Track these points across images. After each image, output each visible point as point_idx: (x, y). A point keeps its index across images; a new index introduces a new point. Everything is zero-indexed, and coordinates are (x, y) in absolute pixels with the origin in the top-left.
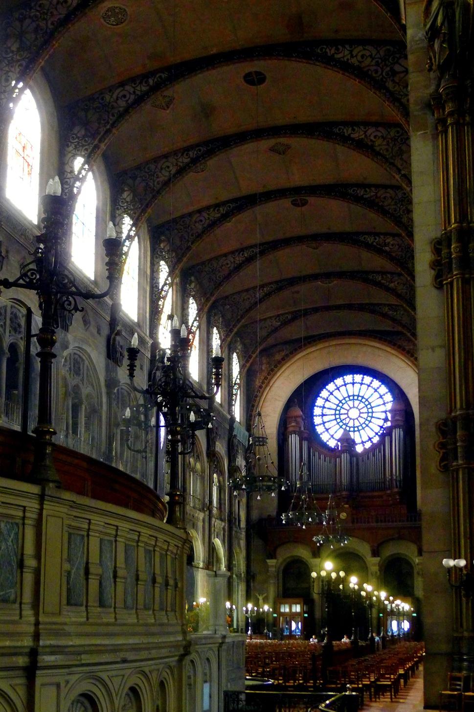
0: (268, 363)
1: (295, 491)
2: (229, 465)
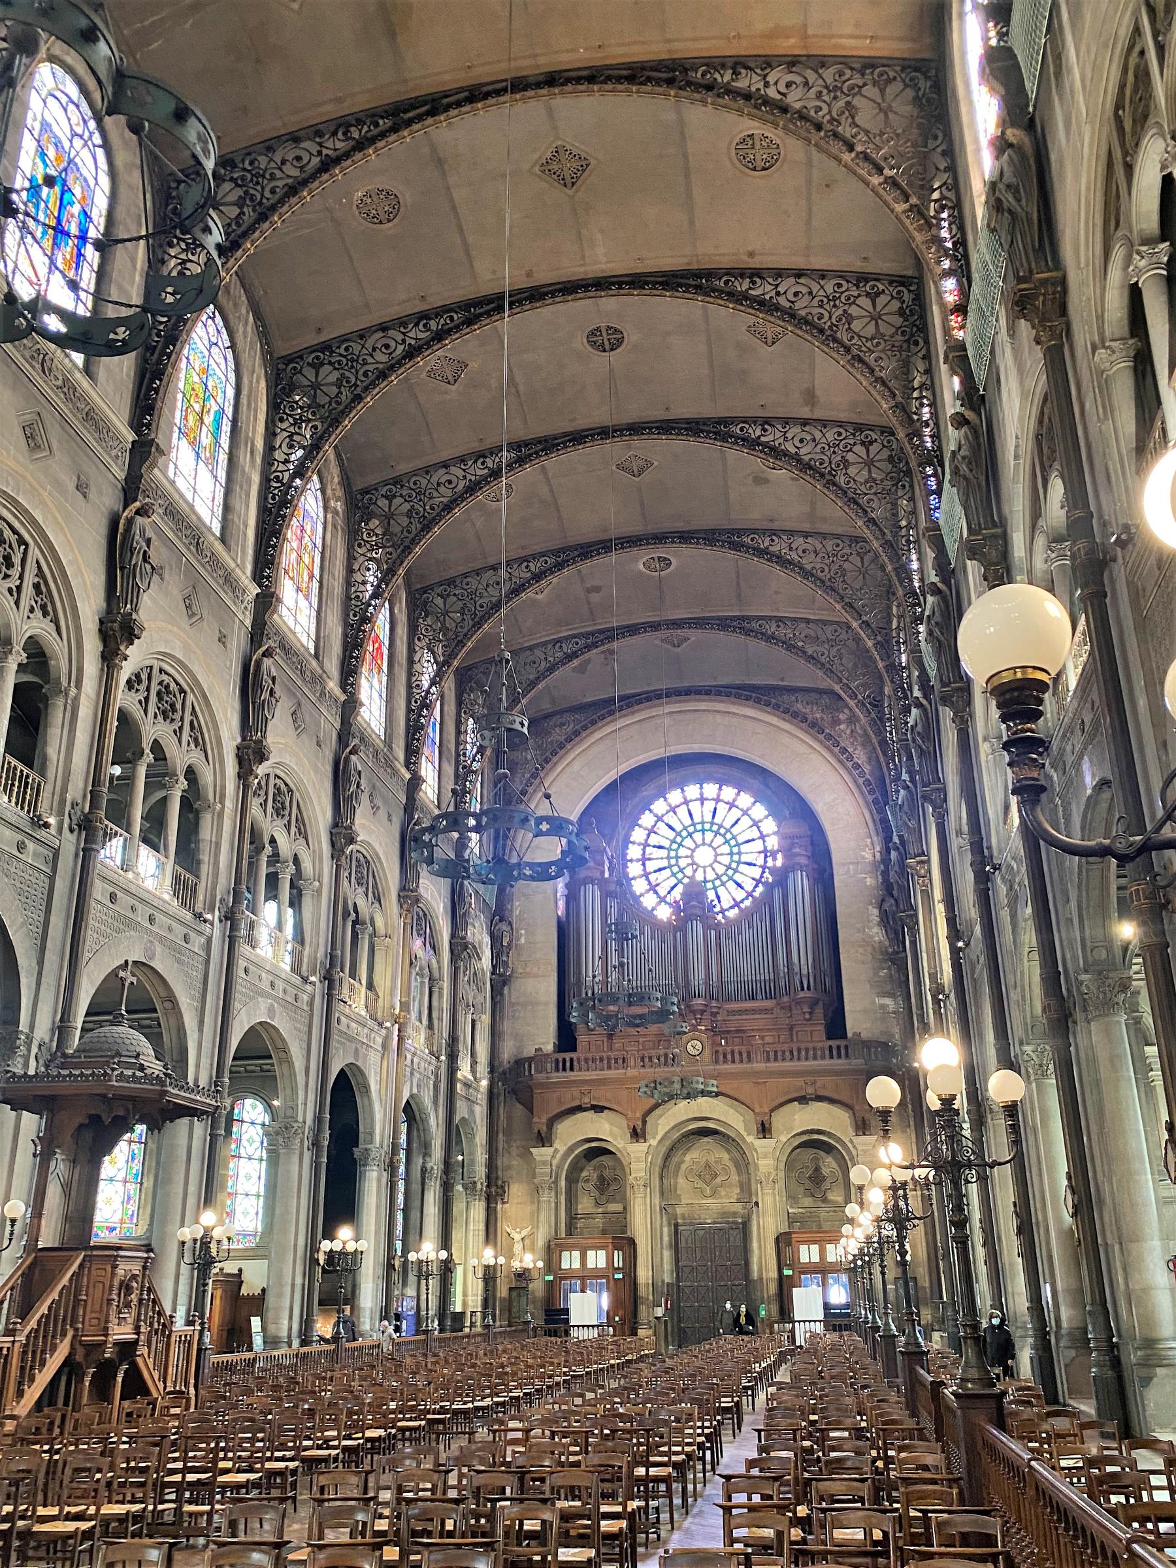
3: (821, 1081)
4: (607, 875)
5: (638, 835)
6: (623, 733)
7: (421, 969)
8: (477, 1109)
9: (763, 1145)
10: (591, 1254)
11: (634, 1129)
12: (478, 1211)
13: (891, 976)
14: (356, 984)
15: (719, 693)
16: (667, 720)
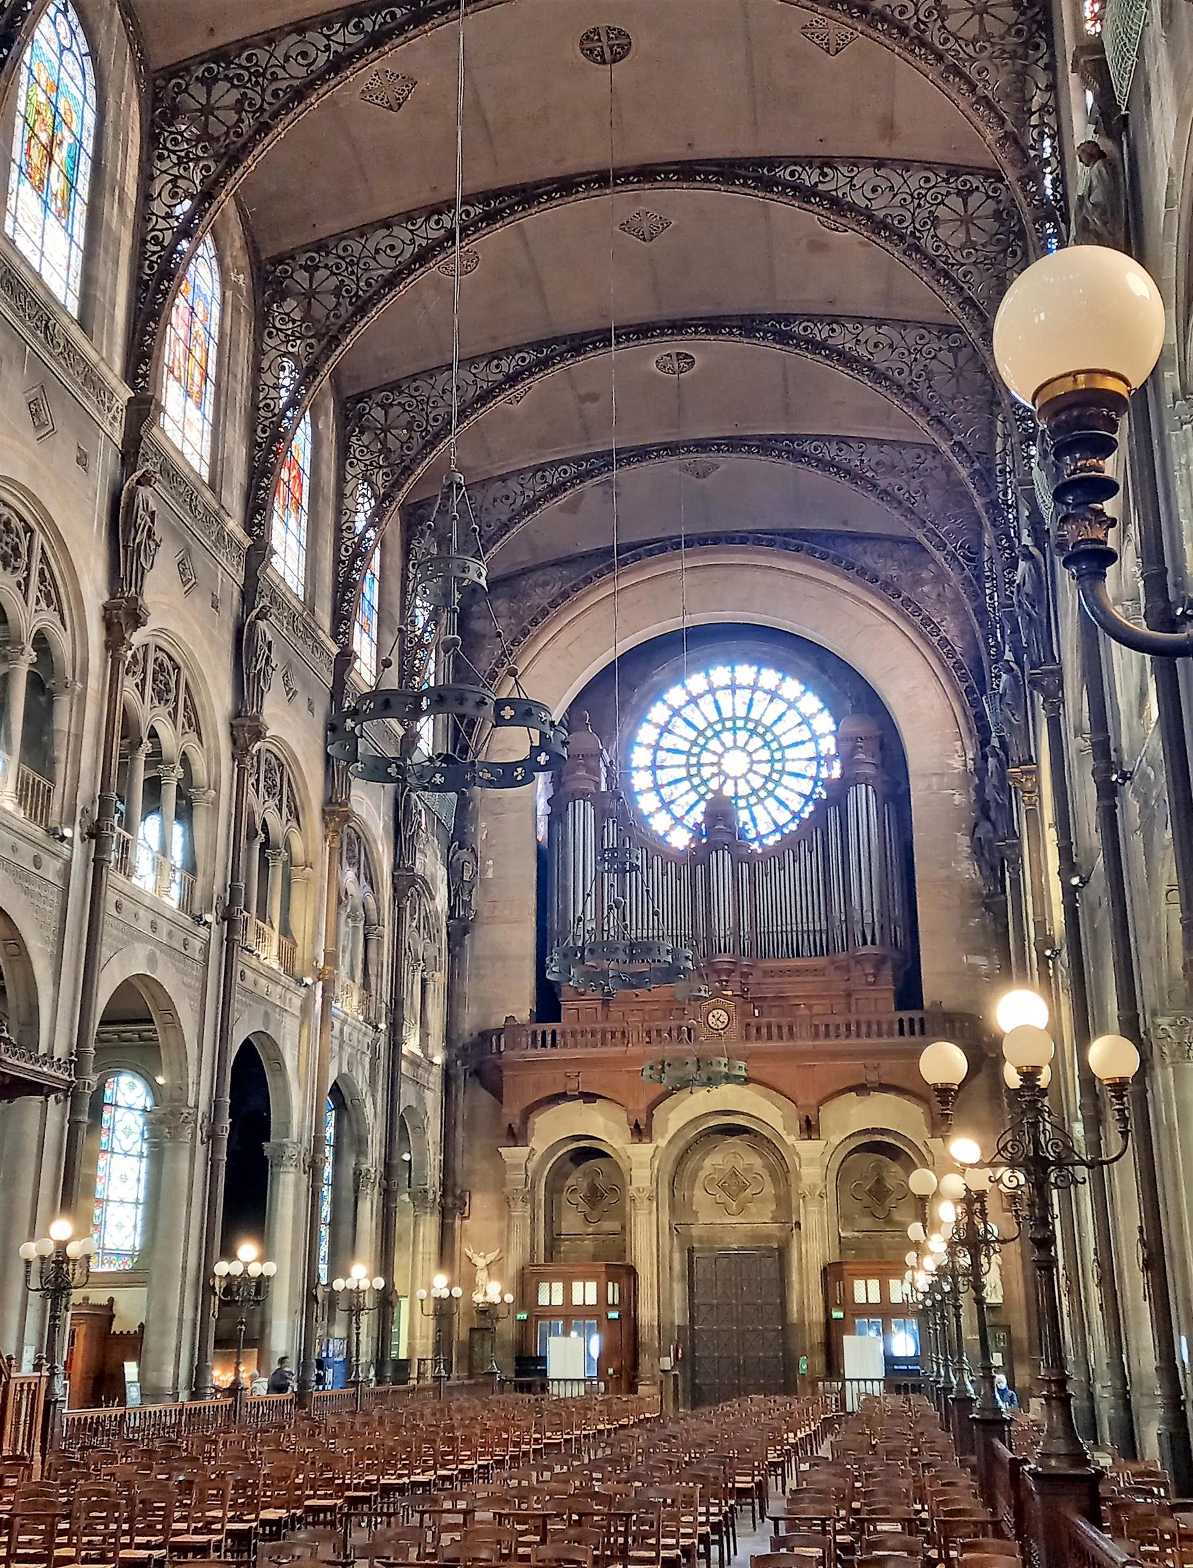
0: (514, 614)
2: (396, 866)
3: (888, 1064)
4: (603, 788)
5: (646, 734)
6: (629, 595)
7: (354, 910)
8: (429, 1095)
9: (808, 1149)
10: (577, 1286)
11: (637, 1126)
12: (429, 1228)
13: (984, 926)
14: (267, 928)
15: (758, 542)
16: (687, 578)
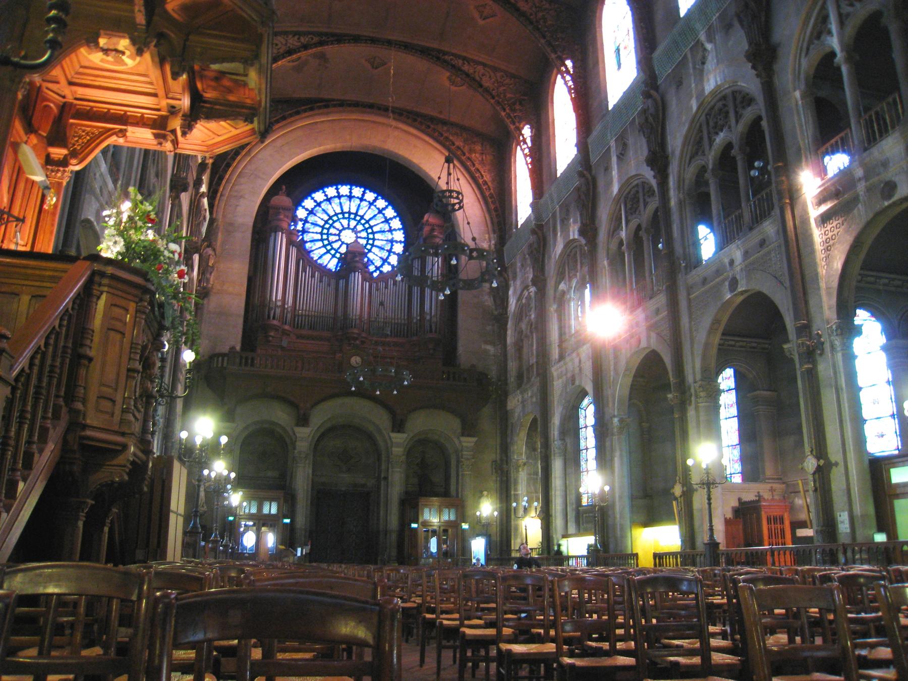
1: (274, 318)
